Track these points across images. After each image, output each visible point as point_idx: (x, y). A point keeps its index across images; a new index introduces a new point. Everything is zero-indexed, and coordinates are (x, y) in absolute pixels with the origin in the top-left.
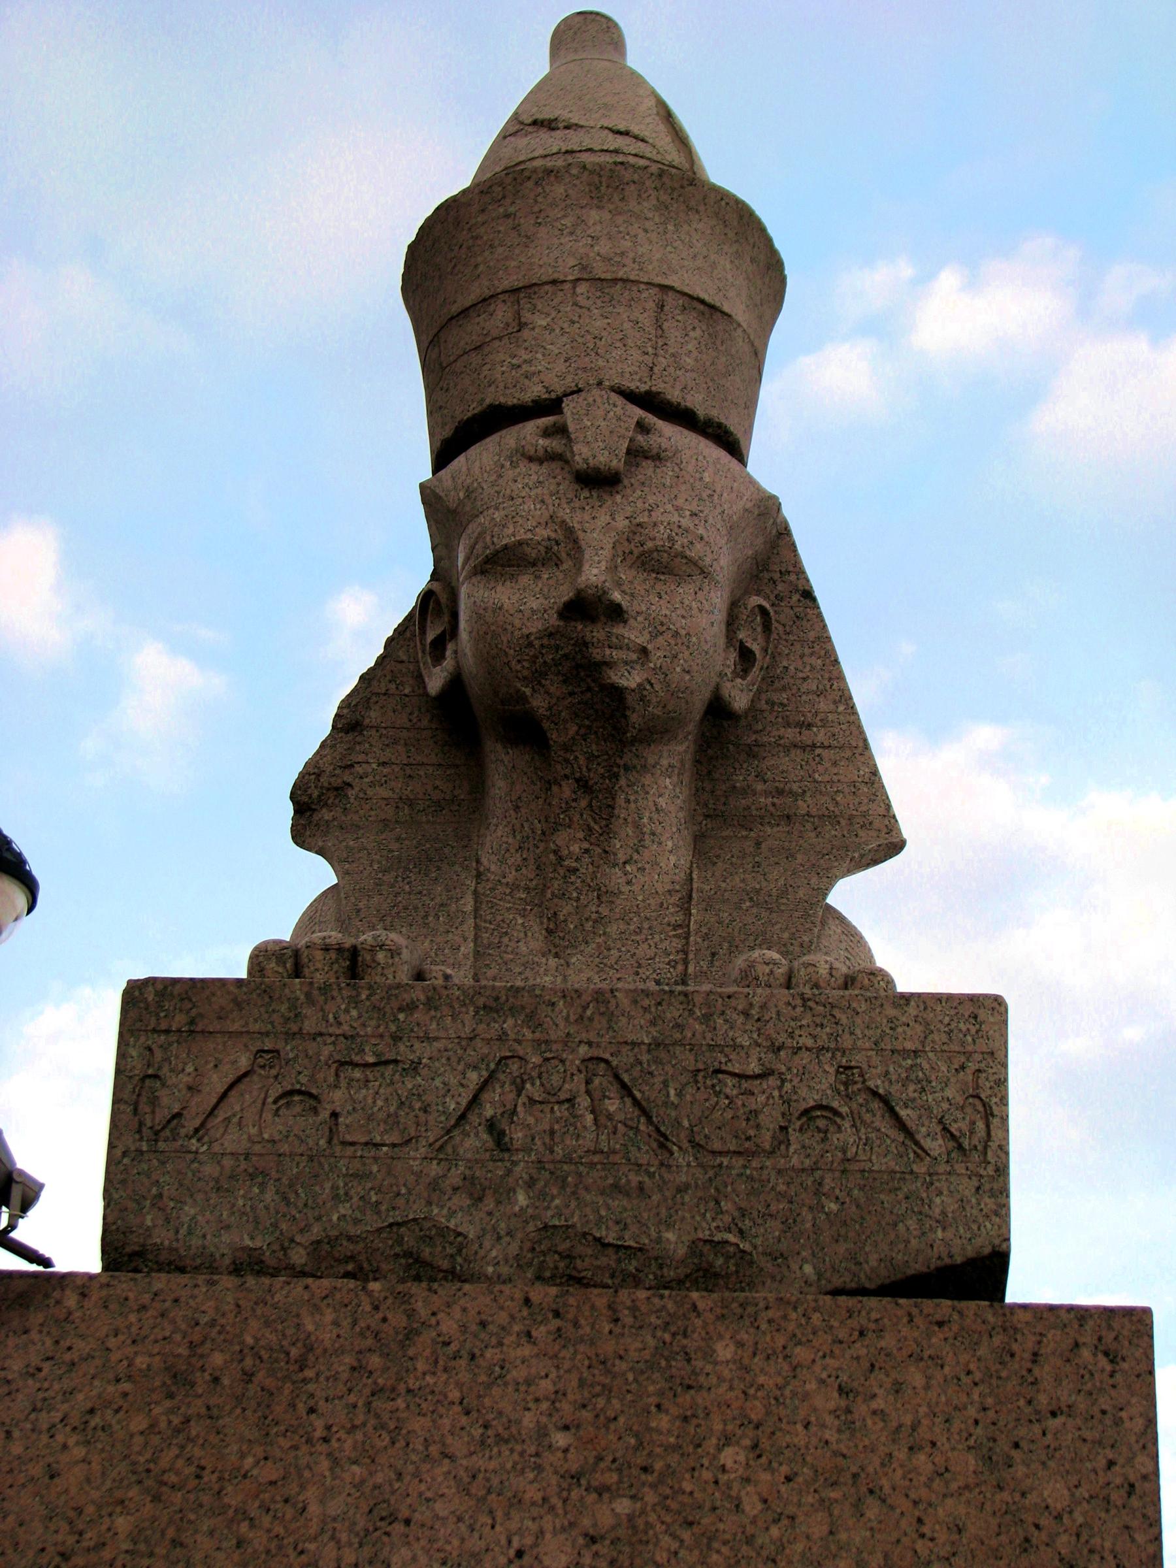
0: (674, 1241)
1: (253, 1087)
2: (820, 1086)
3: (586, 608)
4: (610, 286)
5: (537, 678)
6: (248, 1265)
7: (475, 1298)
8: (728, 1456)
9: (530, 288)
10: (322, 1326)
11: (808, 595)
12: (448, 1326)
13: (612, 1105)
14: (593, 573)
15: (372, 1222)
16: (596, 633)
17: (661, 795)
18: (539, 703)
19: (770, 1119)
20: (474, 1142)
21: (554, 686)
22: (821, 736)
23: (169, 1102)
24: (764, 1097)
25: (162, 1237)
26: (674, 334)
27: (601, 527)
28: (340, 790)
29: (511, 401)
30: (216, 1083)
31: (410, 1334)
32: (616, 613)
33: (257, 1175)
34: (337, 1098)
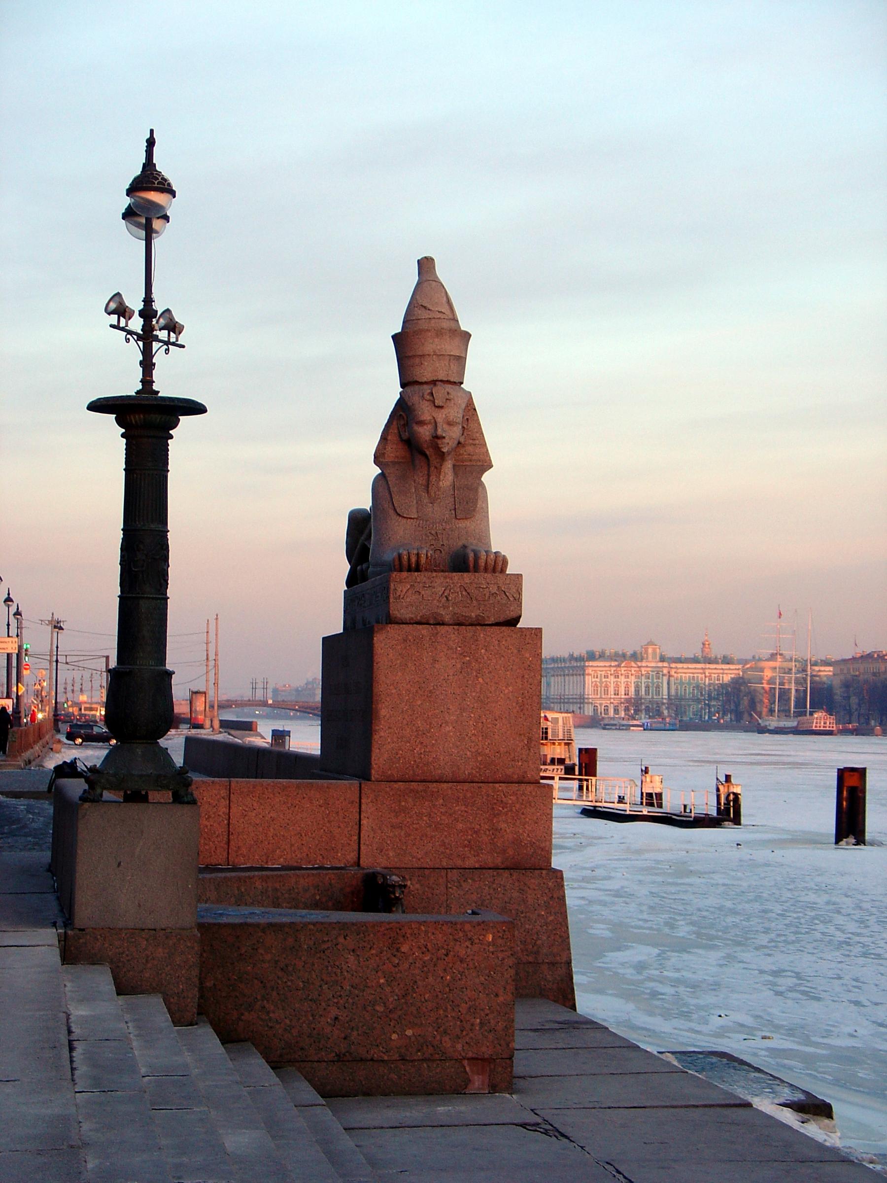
1: (410, 592)
3: (437, 437)
4: (440, 356)
5: (428, 448)
8: (483, 651)
9: (423, 356)
10: (424, 632)
11: (475, 409)
12: (443, 632)
16: (439, 442)
17: (448, 465)
18: (428, 453)
21: (431, 450)
22: (477, 442)
23: (398, 594)
26: (452, 366)
27: (440, 416)
28: (384, 454)
31: (437, 633)
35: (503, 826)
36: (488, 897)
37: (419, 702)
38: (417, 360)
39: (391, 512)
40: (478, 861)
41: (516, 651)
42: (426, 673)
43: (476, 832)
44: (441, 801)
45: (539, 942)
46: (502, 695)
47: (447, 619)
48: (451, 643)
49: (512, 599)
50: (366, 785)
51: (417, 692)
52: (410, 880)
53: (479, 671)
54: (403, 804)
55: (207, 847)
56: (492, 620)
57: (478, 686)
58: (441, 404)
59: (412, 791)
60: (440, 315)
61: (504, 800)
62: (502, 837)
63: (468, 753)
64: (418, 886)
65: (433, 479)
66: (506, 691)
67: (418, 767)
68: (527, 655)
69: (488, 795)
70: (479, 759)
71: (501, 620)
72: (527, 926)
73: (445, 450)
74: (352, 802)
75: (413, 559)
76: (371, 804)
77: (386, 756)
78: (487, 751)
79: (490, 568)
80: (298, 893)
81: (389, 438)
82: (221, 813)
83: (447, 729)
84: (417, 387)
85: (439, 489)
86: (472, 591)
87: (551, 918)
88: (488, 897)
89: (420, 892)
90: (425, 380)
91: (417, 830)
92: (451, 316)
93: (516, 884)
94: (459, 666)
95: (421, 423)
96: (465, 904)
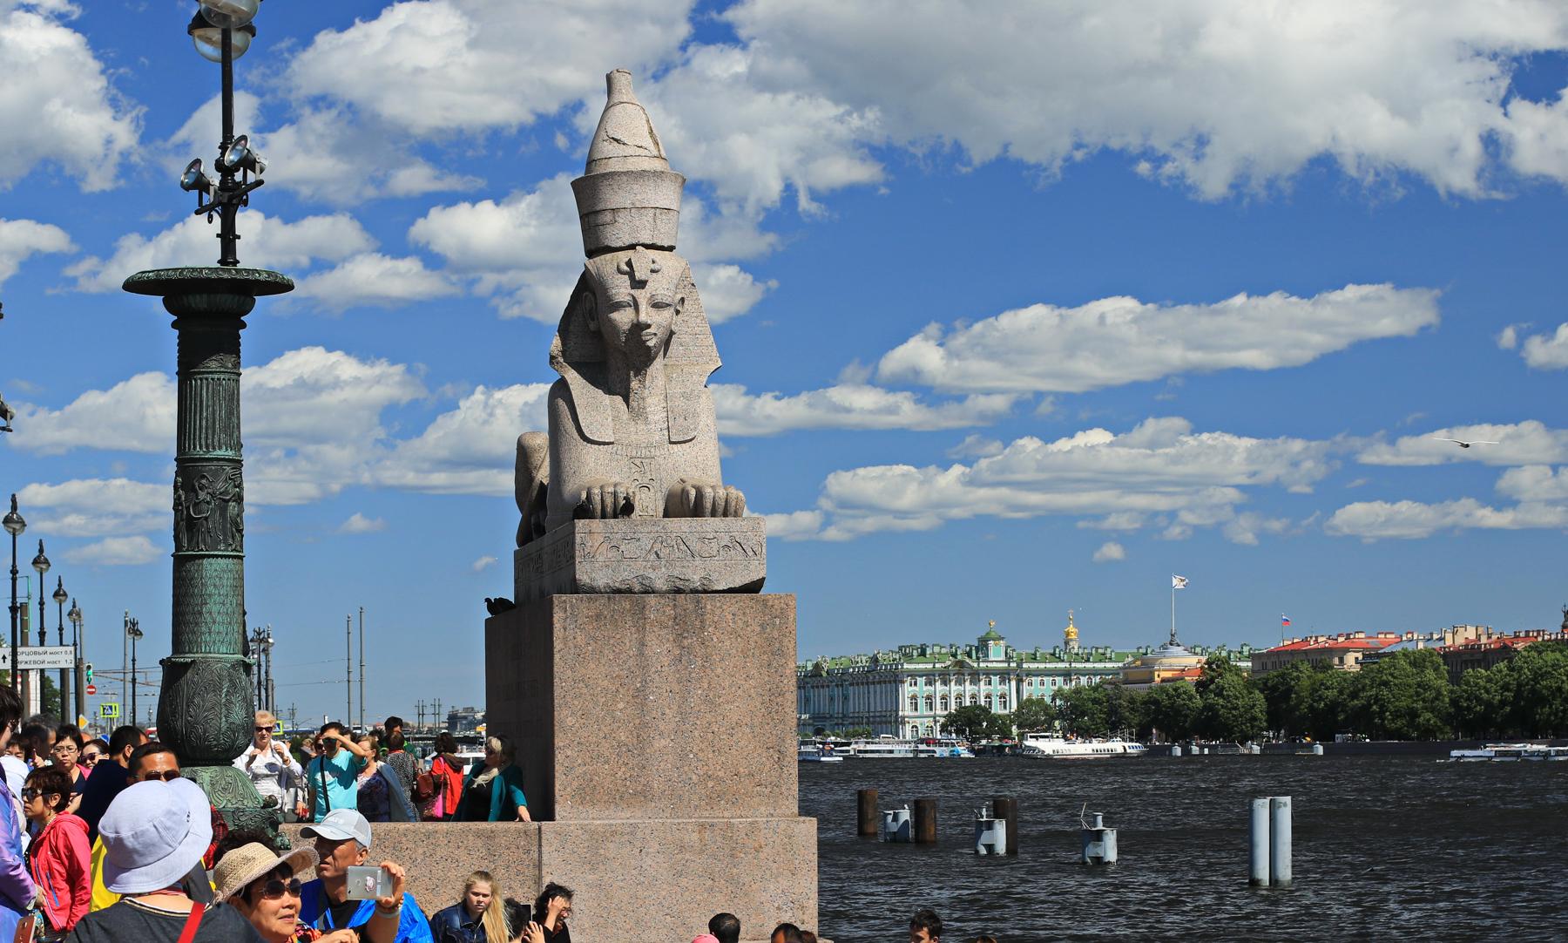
0: (696, 578)
13: (683, 547)
14: (643, 318)
19: (715, 548)
20: (653, 557)
24: (714, 545)
27: (642, 296)
29: (614, 244)
32: (649, 326)
34: (622, 548)
37: (621, 705)
38: (608, 217)
39: (576, 435)
47: (660, 584)
50: (545, 825)
53: (707, 658)
58: (643, 278)
60: (640, 151)
65: (634, 384)
70: (710, 784)
71: (738, 583)
73: (651, 344)
75: (609, 501)
76: (555, 854)
77: (575, 784)
78: (721, 774)
79: (720, 510)
84: (609, 256)
86: (696, 546)
90: (620, 244)
92: (655, 153)
95: (618, 306)
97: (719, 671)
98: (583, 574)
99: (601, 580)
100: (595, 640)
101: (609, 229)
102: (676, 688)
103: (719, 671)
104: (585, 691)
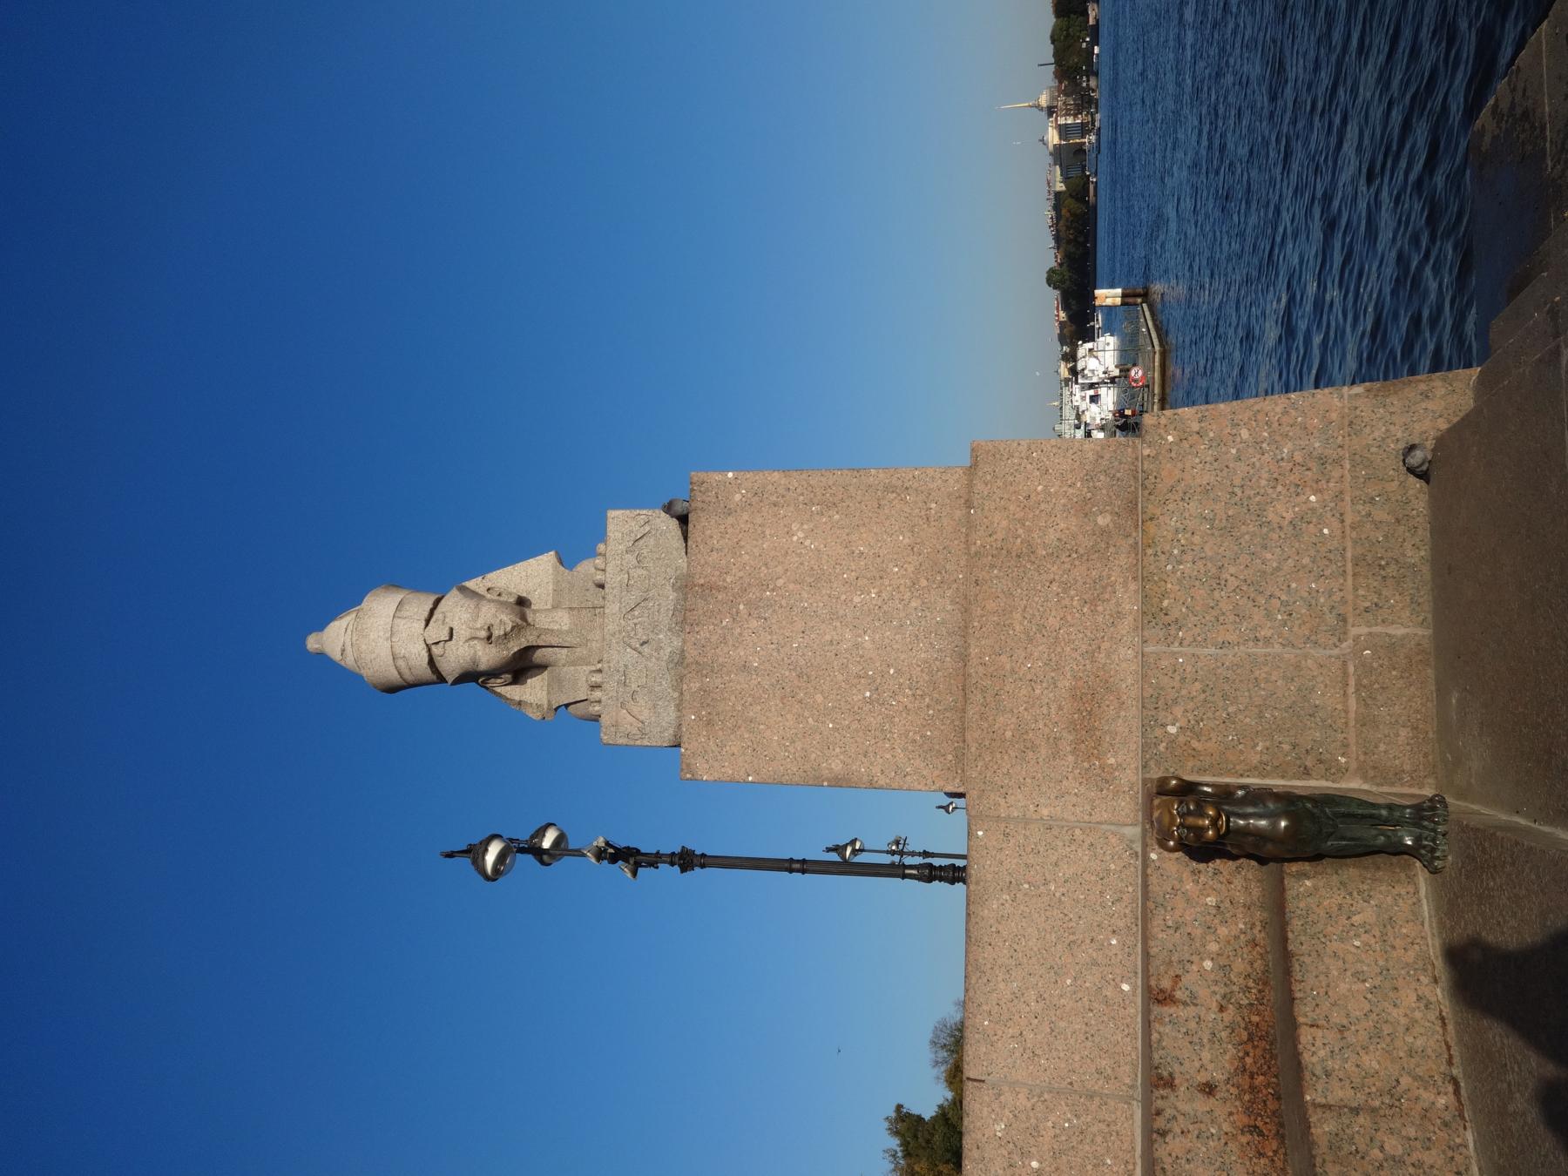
0: (673, 596)
2: (631, 558)
6: (679, 708)
7: (689, 647)
10: (695, 686)
15: (667, 676)
16: (497, 632)
20: (646, 649)
21: (511, 644)
23: (635, 731)
25: (671, 731)
28: (538, 706)
30: (630, 718)
33: (655, 706)
34: (634, 686)
35: (1052, 536)
36: (1200, 564)
37: (819, 698)
38: (401, 663)
40: (1125, 584)
41: (731, 520)
42: (766, 683)
43: (1065, 591)
44: (1004, 658)
45: (1298, 457)
46: (807, 543)
47: (677, 643)
48: (714, 638)
49: (647, 528)
51: (800, 702)
52: (1164, 726)
54: (1009, 734)
55: (1099, 1139)
56: (682, 562)
57: (791, 586)
59: (983, 716)
61: (1000, 536)
62: (1074, 537)
63: (914, 604)
64: (1178, 711)
66: (800, 534)
67: (938, 702)
68: (738, 497)
69: (993, 566)
70: (924, 583)
72: (1263, 482)
74: (1006, 835)
76: (1011, 799)
77: (918, 762)
78: (911, 568)
80: (1199, 1020)
81: (517, 698)
82: (1029, 1105)
83: (868, 645)
85: (569, 632)
87: (1245, 434)
88: (1200, 564)
89: (1191, 705)
91: (1060, 708)
93: (1171, 507)
94: (754, 623)
96: (1214, 613)
97: (780, 569)
98: (660, 735)
99: (669, 715)
100: (737, 727)
101: (412, 663)
102: (800, 626)
103: (780, 569)
104: (799, 745)
